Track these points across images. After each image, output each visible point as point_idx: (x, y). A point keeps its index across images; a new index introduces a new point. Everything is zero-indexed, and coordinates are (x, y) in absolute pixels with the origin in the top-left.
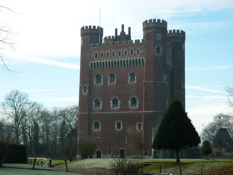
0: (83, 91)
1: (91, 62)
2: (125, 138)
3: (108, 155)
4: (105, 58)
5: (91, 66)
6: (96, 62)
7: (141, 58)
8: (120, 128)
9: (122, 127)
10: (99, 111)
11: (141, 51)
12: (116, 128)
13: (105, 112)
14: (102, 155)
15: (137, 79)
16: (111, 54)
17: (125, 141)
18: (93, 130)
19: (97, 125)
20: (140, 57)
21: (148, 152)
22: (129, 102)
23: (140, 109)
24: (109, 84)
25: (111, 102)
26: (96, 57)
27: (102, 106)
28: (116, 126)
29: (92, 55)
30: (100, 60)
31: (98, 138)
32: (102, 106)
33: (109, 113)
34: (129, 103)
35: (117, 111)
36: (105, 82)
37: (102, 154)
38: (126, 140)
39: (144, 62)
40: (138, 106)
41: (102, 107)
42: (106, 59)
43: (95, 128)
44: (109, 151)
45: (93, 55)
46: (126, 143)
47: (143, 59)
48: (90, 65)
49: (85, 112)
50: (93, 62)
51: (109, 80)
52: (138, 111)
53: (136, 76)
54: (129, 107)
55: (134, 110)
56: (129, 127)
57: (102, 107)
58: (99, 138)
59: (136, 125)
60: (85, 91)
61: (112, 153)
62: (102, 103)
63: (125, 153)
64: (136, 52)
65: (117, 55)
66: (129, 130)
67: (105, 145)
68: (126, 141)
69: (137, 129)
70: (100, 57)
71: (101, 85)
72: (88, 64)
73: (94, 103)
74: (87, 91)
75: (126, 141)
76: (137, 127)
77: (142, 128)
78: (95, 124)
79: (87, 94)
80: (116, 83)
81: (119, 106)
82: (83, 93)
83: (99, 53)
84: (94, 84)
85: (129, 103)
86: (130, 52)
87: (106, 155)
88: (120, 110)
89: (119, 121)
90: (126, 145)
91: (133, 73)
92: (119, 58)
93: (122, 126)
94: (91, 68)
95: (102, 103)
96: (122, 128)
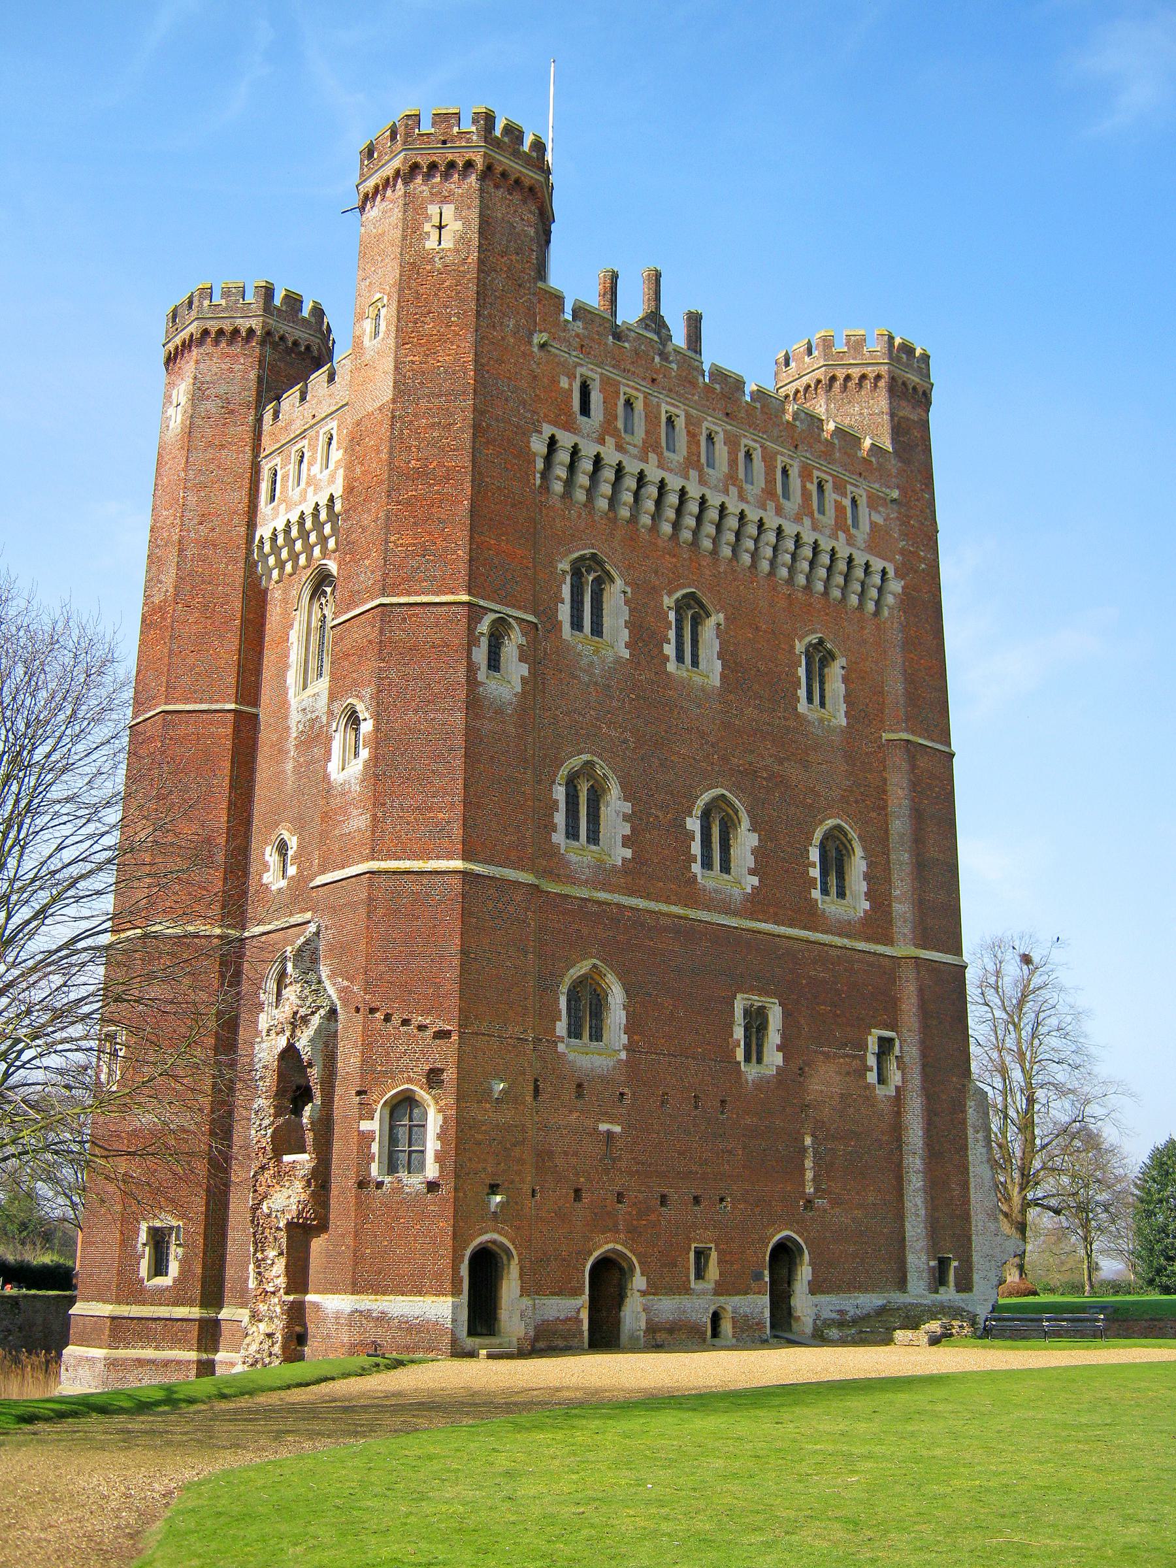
0: (480, 655)
1: (548, 430)
2: (804, 1150)
3: (686, 1290)
4: (650, 446)
5: (540, 465)
6: (589, 449)
7: (877, 564)
8: (759, 1060)
9: (779, 1048)
10: (604, 877)
11: (879, 520)
12: (740, 1054)
13: (648, 897)
14: (644, 1293)
15: (848, 698)
16: (692, 436)
17: (802, 1170)
18: (561, 1047)
19: (588, 1010)
20: (871, 548)
21: (955, 1264)
22: (814, 855)
23: (878, 924)
24: (671, 667)
25: (693, 824)
26: (585, 410)
27: (627, 842)
28: (739, 1033)
29: (554, 381)
30: (620, 448)
31: (603, 1127)
32: (627, 842)
33: (692, 914)
34: (813, 865)
35: (735, 913)
36: (644, 636)
37: (639, 1281)
38: (809, 1163)
39: (890, 600)
40: (866, 905)
41: (628, 853)
42: (660, 455)
43: (574, 1032)
44: (692, 1255)
45: (564, 383)
46: (810, 1189)
47: (884, 572)
48: (539, 446)
49: (517, 865)
50: (566, 440)
51: (672, 634)
52: (868, 939)
53: (835, 671)
54: (816, 894)
55: (843, 929)
56: (827, 1055)
57: (628, 853)
58: (617, 1129)
59: (865, 1047)
60: (494, 663)
61: (713, 1271)
62: (626, 817)
63: (804, 1273)
64: (847, 502)
65: (733, 463)
66: (824, 1081)
67: (664, 1200)
68: (809, 1175)
69: (872, 1077)
70: (620, 425)
71: (618, 660)
72: (526, 435)
73: (560, 793)
74: (515, 670)
75: (809, 1175)
76: (872, 1061)
77: (895, 1078)
78: (573, 997)
79: (524, 693)
80: (723, 676)
81: (752, 872)
82: (481, 676)
83: (610, 387)
84: (558, 625)
85: (813, 865)
86: (813, 488)
87: (671, 1291)
88: (756, 905)
89: (757, 1000)
90: (809, 1202)
91: (821, 642)
92: (750, 498)
93: (773, 1037)
94: (538, 482)
95: (626, 817)
96: (774, 1058)
